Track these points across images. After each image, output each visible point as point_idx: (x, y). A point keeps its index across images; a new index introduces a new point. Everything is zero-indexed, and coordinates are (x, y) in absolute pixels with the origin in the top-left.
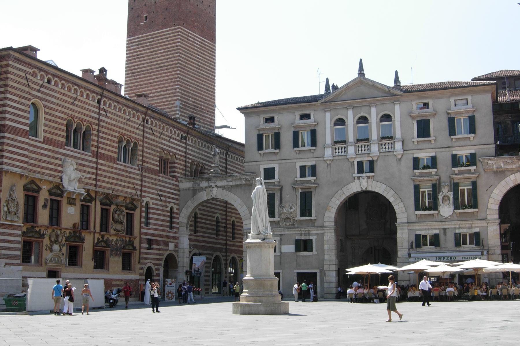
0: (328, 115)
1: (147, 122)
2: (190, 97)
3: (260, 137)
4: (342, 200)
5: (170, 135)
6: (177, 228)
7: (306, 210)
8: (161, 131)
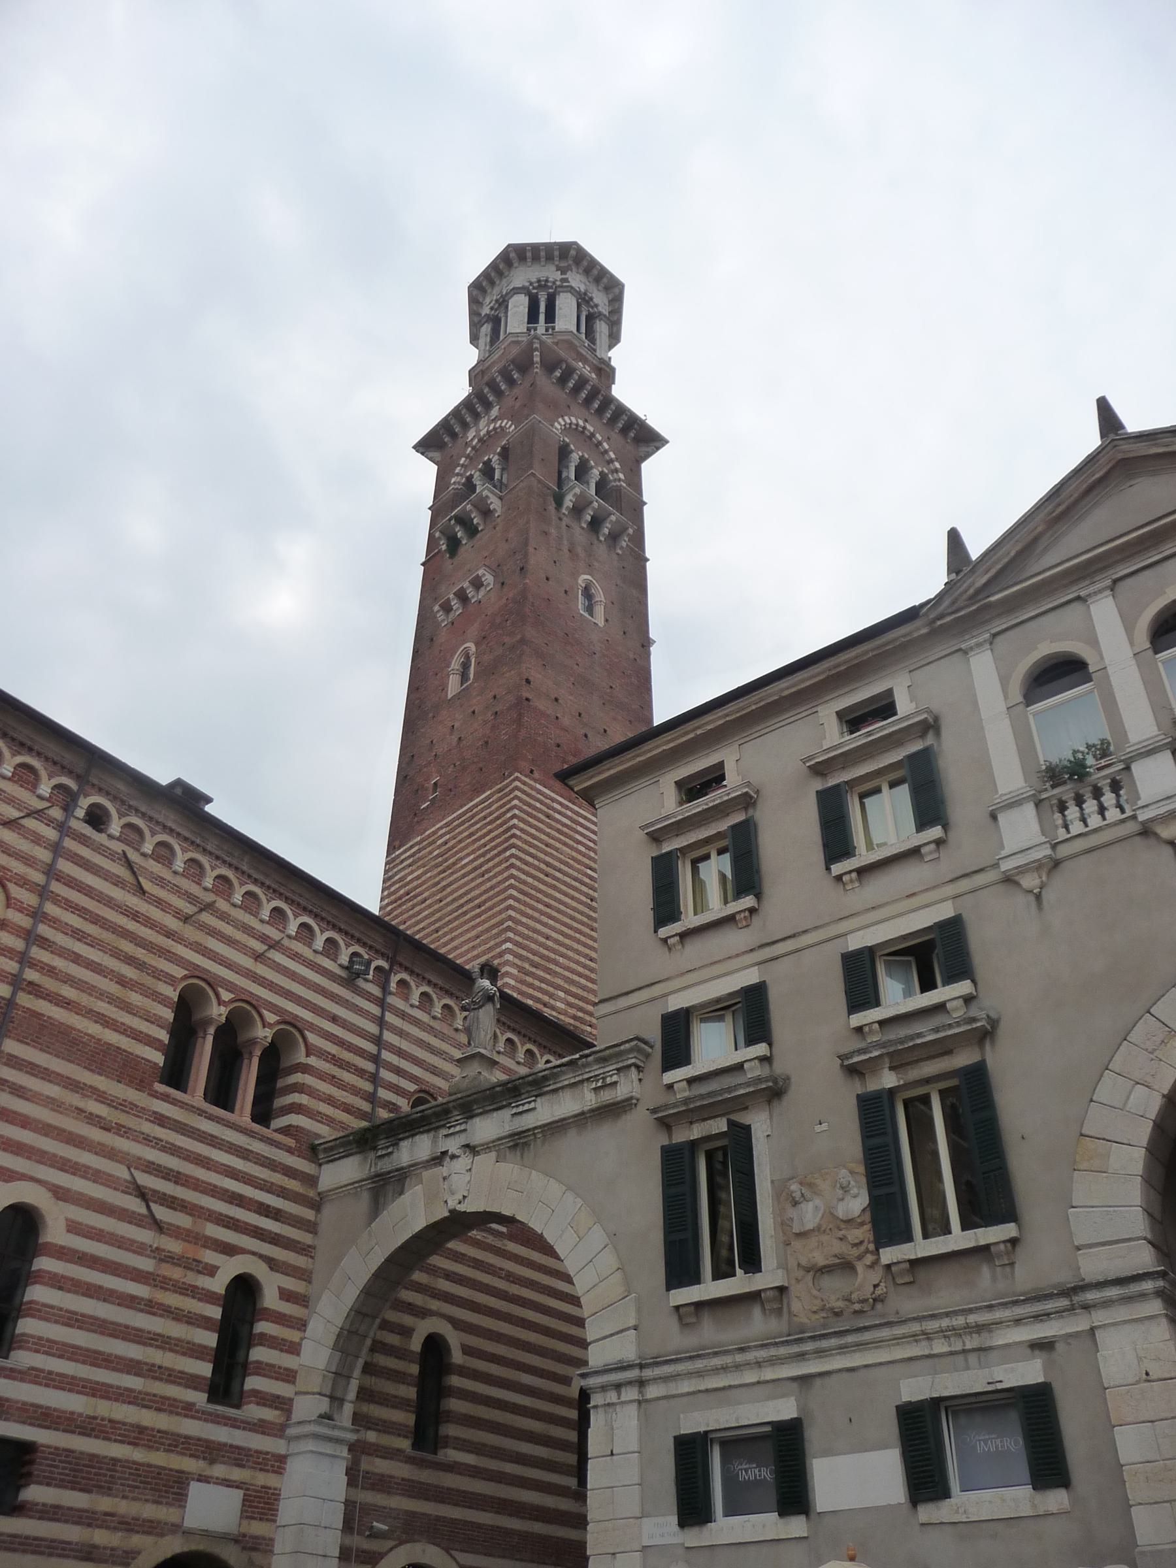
1: (96, 818)
2: (558, 987)
5: (273, 933)
6: (282, 1404)
8: (209, 898)
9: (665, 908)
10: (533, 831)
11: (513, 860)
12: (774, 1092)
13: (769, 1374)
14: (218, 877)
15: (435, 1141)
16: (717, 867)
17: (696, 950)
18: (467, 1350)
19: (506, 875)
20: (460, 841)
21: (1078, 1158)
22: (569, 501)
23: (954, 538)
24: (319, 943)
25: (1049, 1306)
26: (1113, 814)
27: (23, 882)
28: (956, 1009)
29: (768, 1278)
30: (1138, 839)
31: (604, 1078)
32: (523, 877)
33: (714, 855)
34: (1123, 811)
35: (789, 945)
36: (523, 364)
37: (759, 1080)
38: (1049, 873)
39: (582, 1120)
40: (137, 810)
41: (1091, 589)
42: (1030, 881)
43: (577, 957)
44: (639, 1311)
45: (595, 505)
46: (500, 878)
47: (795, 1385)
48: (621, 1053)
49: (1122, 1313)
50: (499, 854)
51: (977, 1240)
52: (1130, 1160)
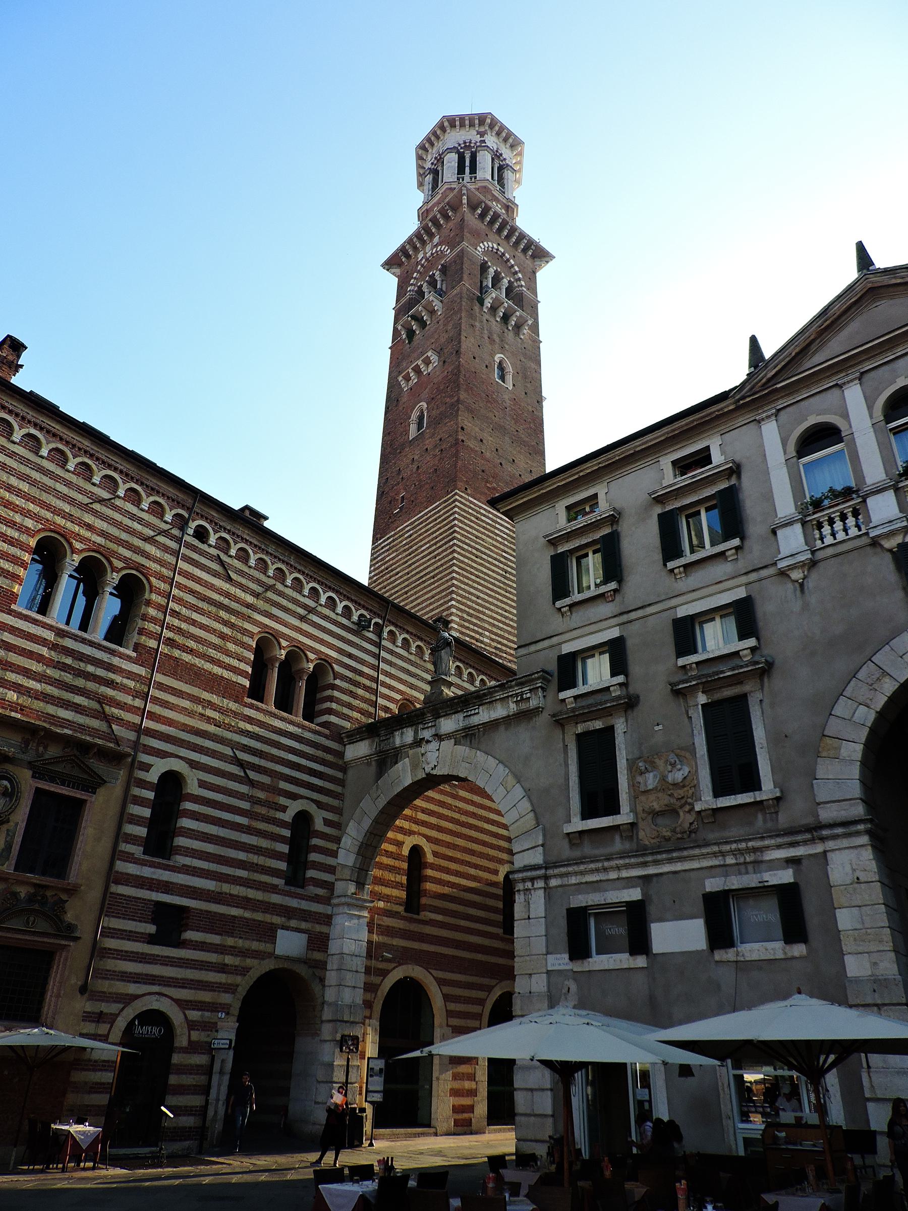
0: (770, 431)
1: (201, 535)
3: (559, 565)
4: (880, 701)
7: (734, 766)
8: (271, 582)
9: (560, 588)
10: (468, 528)
11: (455, 548)
12: (630, 704)
13: (625, 874)
14: (277, 569)
15: (416, 733)
16: (593, 562)
17: (578, 617)
18: (435, 854)
19: (450, 557)
20: (420, 535)
21: (820, 749)
22: (488, 303)
23: (754, 341)
24: (339, 609)
25: (799, 838)
26: (854, 531)
27: (161, 577)
28: (746, 656)
29: (624, 817)
30: (868, 548)
31: (522, 695)
32: (462, 558)
33: (590, 554)
34: (860, 530)
35: (640, 613)
36: (455, 206)
37: (619, 698)
38: (809, 570)
39: (507, 721)
40: (225, 529)
41: (845, 380)
42: (796, 575)
43: (496, 609)
44: (544, 836)
45: (506, 305)
46: (446, 559)
47: (640, 881)
48: (533, 680)
49: (845, 843)
50: (446, 543)
51: (755, 798)
52: (854, 751)
